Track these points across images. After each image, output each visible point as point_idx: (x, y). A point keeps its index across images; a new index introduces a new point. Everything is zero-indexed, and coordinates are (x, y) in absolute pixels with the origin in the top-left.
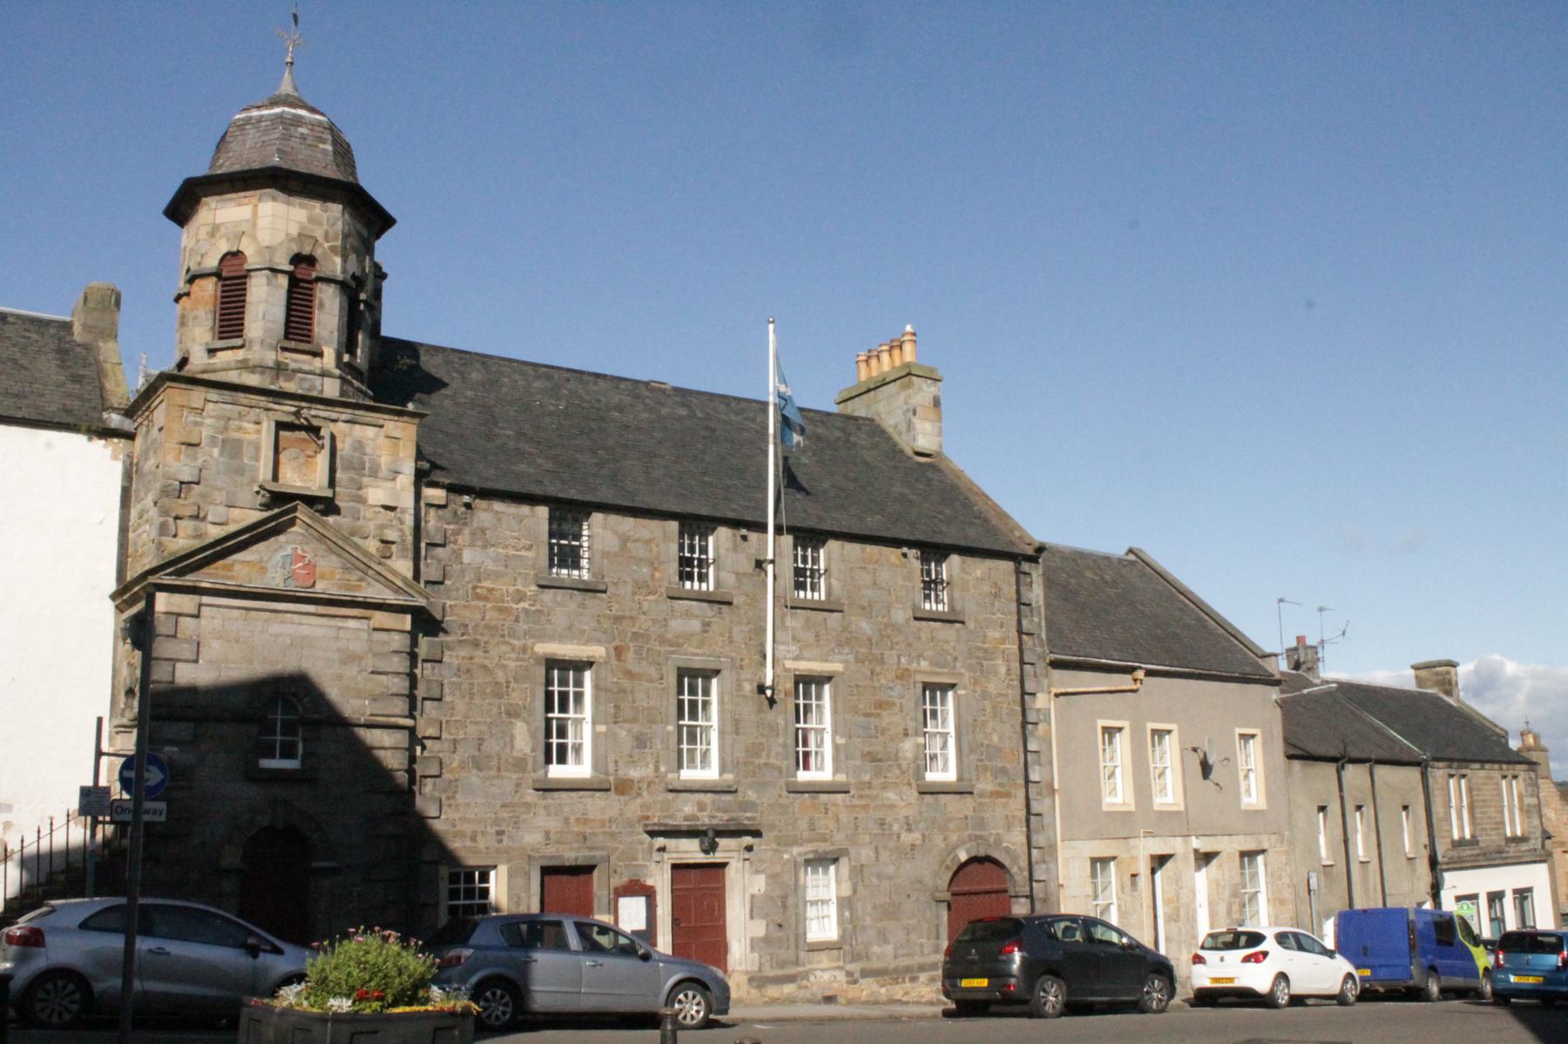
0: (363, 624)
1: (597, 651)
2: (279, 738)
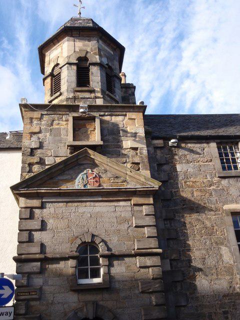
0: (128, 203)
2: (89, 267)
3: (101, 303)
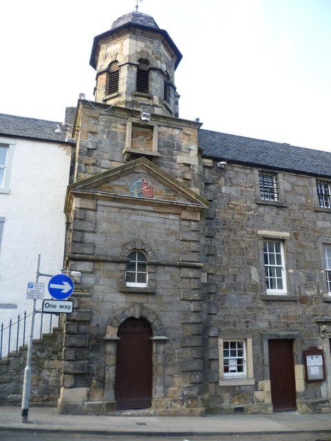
0: (177, 217)
1: (286, 234)
2: (136, 272)
3: (146, 305)
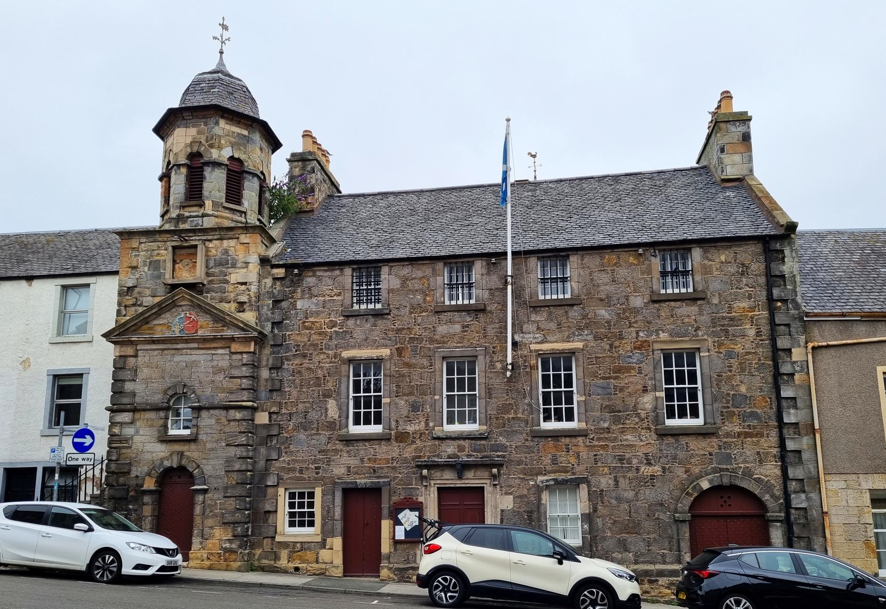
1: (385, 352)
3: (187, 454)
